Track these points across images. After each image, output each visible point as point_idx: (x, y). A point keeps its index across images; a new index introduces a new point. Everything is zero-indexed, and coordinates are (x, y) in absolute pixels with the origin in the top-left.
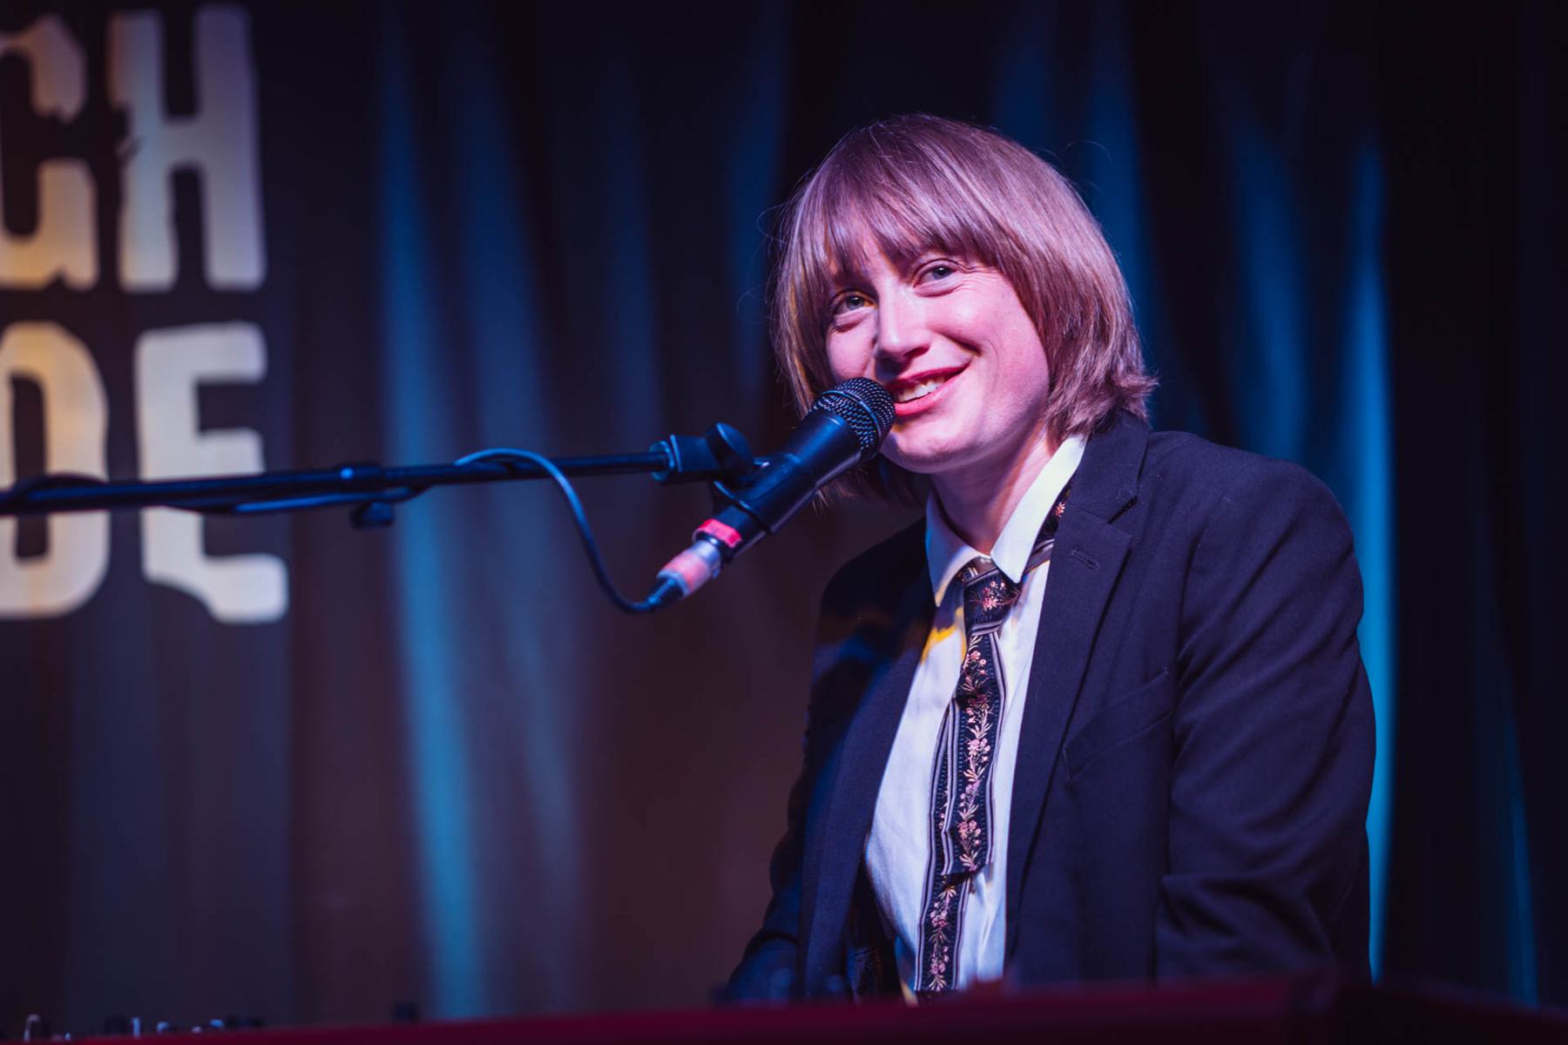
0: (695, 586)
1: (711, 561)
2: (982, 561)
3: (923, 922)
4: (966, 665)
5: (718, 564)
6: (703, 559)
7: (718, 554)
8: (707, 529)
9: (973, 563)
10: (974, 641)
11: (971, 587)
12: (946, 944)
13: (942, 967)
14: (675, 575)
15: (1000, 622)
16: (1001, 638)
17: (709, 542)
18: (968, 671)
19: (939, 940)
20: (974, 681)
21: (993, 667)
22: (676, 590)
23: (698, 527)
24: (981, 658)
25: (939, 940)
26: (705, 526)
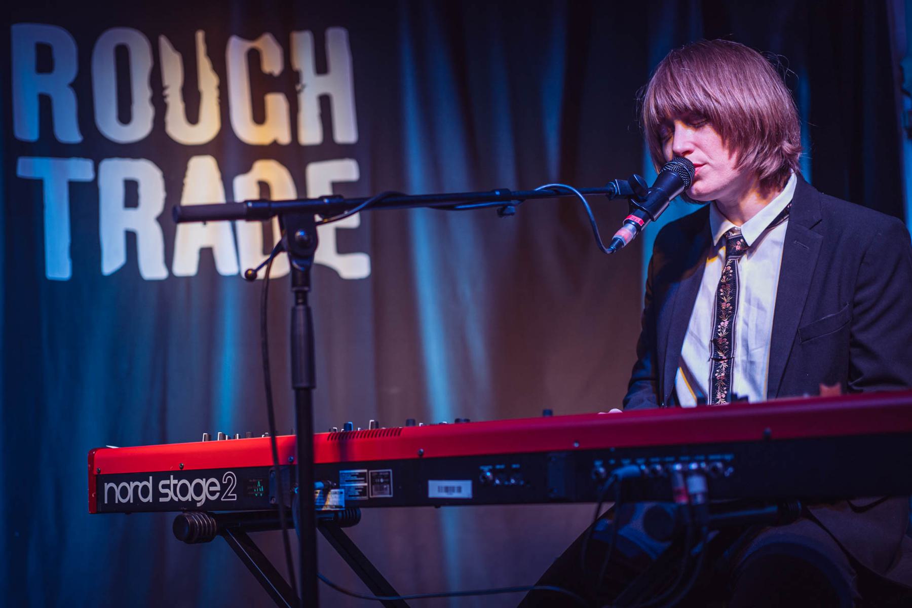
0: (629, 241)
1: (633, 231)
2: (736, 229)
3: (711, 378)
4: (724, 271)
5: (635, 233)
6: (630, 230)
7: (635, 228)
8: (630, 219)
9: (732, 230)
10: (729, 262)
11: (730, 240)
12: (725, 386)
13: (724, 396)
14: (621, 238)
15: (740, 256)
16: (740, 262)
17: (631, 223)
18: (725, 274)
19: (721, 385)
20: (726, 279)
21: (735, 273)
22: (621, 243)
23: (626, 218)
24: (731, 269)
25: (721, 385)
26: (629, 217)
